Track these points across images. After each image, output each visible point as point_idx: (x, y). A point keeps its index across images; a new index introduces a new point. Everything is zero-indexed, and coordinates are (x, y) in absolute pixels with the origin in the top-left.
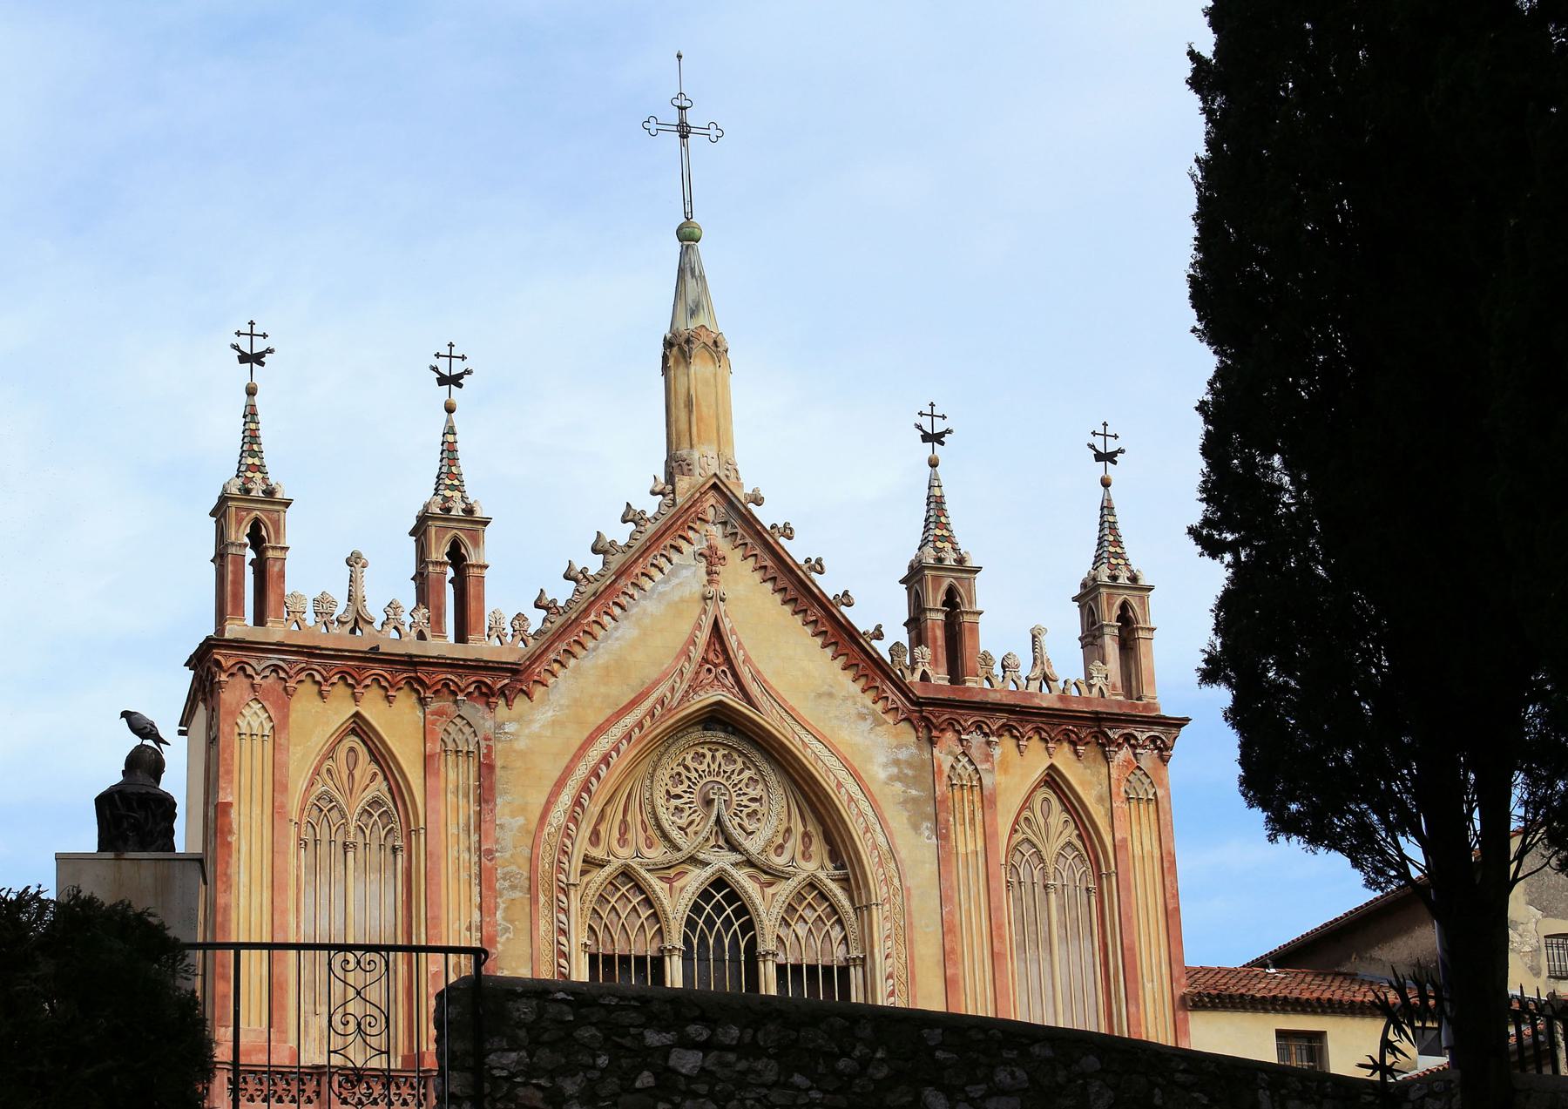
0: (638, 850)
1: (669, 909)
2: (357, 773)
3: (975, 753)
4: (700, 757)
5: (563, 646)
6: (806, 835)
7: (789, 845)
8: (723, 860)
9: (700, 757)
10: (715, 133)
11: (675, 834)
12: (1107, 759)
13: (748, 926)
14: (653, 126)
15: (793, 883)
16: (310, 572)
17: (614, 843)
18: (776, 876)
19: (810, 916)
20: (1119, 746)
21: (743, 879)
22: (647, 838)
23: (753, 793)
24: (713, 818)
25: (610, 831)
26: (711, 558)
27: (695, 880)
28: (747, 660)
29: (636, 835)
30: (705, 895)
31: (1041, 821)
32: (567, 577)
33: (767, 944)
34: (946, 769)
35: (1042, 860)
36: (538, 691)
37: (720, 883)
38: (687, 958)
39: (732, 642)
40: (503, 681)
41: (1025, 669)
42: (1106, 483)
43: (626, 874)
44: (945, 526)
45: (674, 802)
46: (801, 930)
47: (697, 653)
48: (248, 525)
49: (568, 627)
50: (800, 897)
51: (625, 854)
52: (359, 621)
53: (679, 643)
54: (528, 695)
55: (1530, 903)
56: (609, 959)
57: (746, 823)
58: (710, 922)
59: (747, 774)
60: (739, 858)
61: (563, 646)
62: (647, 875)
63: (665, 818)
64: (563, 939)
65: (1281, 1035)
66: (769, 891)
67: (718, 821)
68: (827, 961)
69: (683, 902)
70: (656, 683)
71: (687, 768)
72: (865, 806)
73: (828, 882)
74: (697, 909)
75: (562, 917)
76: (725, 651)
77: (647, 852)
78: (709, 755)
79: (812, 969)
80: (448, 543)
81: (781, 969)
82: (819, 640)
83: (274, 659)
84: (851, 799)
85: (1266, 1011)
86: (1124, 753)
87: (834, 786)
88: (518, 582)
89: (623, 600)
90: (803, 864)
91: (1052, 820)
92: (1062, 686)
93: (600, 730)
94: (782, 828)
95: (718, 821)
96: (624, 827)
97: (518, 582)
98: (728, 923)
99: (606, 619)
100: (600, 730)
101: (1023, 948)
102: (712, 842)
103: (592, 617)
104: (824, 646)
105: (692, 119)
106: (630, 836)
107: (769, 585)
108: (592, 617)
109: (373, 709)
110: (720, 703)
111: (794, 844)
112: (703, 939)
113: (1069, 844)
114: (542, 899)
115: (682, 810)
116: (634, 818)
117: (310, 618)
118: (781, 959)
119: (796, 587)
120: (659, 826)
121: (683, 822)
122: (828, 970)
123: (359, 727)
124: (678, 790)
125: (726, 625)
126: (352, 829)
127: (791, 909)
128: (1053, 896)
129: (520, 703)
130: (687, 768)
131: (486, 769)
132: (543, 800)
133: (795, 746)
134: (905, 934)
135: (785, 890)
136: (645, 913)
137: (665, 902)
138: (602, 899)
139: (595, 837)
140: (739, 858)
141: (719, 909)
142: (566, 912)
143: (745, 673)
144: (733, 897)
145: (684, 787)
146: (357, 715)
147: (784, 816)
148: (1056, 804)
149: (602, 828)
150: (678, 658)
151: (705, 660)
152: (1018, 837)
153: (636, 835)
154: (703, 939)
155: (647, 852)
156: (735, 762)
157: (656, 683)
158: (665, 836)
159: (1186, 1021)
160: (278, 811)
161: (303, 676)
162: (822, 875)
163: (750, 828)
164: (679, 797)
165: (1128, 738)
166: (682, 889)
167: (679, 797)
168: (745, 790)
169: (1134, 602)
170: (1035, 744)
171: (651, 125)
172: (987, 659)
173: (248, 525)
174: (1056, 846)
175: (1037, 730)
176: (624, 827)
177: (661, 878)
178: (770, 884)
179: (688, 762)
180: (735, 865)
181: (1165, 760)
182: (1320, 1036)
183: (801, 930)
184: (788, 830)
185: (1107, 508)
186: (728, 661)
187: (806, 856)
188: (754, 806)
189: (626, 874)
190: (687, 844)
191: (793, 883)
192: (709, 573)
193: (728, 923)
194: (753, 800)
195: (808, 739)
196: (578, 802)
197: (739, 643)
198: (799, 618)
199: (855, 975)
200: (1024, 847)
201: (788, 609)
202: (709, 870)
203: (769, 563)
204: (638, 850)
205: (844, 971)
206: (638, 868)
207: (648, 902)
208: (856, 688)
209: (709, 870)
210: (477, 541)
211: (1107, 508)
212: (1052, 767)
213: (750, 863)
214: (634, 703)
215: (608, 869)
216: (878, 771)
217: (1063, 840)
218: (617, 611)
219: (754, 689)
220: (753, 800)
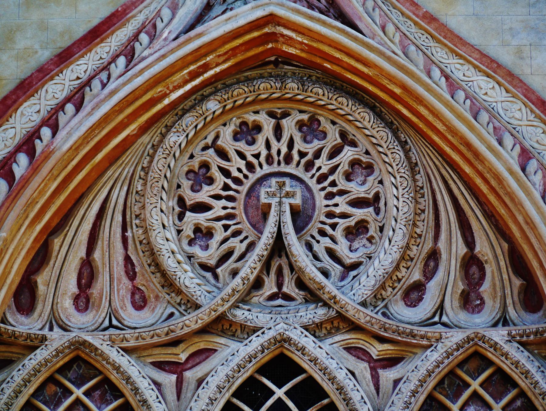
0: (112, 313)
4: (248, 132)
6: (472, 265)
8: (286, 324)
9: (248, 132)
11: (188, 279)
15: (434, 356)
17: (67, 303)
18: (400, 349)
21: (328, 359)
22: (135, 290)
23: (357, 189)
25: (59, 283)
27: (231, 361)
29: (112, 285)
37: (280, 365)
43: (80, 363)
45: (192, 218)
51: (82, 325)
57: (342, 247)
60: (317, 314)
62: (123, 360)
66: (387, 375)
67: (279, 247)
71: (223, 154)
73: (516, 353)
77: (131, 316)
78: (268, 124)
87: (513, 159)
90: (462, 317)
94: (419, 252)
95: (279, 247)
96: (87, 274)
102: (270, 287)
106: (102, 283)
111: (448, 276)
115: (209, 234)
116: (110, 256)
121: (210, 256)
124: (204, 195)
130: (223, 154)
133: (433, 94)
140: (317, 314)
145: (216, 188)
147: (425, 227)
149: (41, 280)
155: (131, 316)
156: (324, 135)
158: (169, 284)
162: (499, 335)
163: (350, 258)
166: (200, 382)
168: (343, 184)
176: (87, 274)
177: (159, 365)
178: (391, 362)
179: (226, 141)
180: (314, 329)
184: (434, 255)
187: (470, 301)
188: (359, 213)
190: (213, 301)
191: (434, 356)
195: (460, 70)
202: (256, 342)
204: (112, 313)
206: (105, 348)
209: (256, 342)
213: (342, 322)
215: (41, 355)
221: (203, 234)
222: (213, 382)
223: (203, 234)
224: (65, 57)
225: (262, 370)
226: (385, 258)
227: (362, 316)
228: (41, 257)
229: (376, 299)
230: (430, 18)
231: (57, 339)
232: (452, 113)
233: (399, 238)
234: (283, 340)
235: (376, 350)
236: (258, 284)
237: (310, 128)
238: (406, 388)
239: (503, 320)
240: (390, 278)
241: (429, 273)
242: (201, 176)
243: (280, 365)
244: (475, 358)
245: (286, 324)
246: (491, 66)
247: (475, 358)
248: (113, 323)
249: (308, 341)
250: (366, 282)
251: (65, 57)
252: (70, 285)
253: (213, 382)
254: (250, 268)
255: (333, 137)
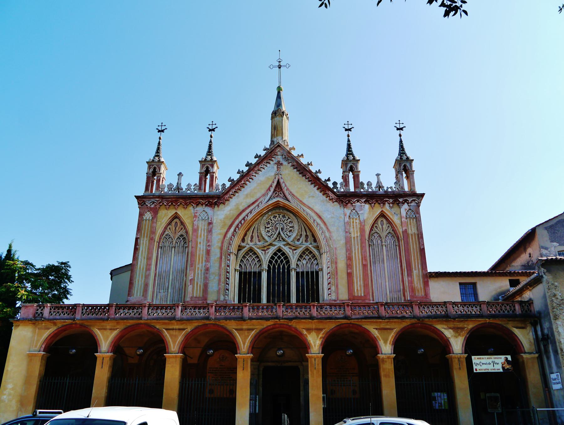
1: (263, 258)
2: (177, 228)
3: (357, 209)
5: (234, 190)
6: (307, 236)
7: (301, 239)
8: (281, 244)
9: (275, 217)
10: (288, 66)
11: (266, 238)
12: (400, 208)
13: (288, 262)
14: (272, 67)
15: (301, 249)
16: (168, 178)
19: (307, 258)
20: (404, 204)
21: (286, 249)
23: (290, 225)
24: (277, 232)
25: (248, 238)
26: (279, 164)
27: (272, 250)
28: (288, 189)
29: (256, 239)
30: (275, 254)
31: (381, 227)
32: (238, 173)
33: (293, 265)
34: (348, 214)
35: (381, 237)
36: (227, 203)
37: (279, 250)
38: (269, 272)
39: (283, 185)
40: (215, 200)
41: (374, 185)
42: (400, 135)
43: (251, 250)
44: (351, 151)
46: (304, 262)
47: (272, 190)
48: (154, 170)
49: (236, 185)
50: (304, 253)
51: (251, 244)
52: (178, 188)
53: (268, 186)
54: (224, 204)
55: (552, 242)
56: (245, 273)
57: (288, 233)
58: (276, 261)
59: (289, 220)
60: (285, 243)
61: (234, 190)
62: (257, 249)
63: (263, 233)
64: (228, 268)
65: (460, 284)
66: (295, 252)
67: (279, 233)
68: (312, 270)
69: (268, 256)
70: (260, 198)
72: (322, 225)
73: (313, 248)
74: (272, 258)
75: (228, 262)
76: (281, 188)
77: (258, 243)
78: (278, 216)
79: (307, 273)
80: (207, 167)
81: (297, 273)
82: (310, 183)
83: (153, 200)
84: (318, 224)
85: (455, 277)
86: (406, 206)
88: (223, 176)
89: (252, 177)
91: (384, 226)
92: (385, 189)
93: (243, 211)
95: (279, 233)
97: (223, 176)
98: (282, 261)
99: (247, 182)
100: (243, 211)
101: (375, 263)
102: (278, 239)
103: (243, 182)
104: (311, 184)
105: (281, 64)
106: (254, 238)
107: (295, 170)
108: (243, 182)
109: (181, 212)
110: (278, 201)
111: (303, 238)
112: (274, 266)
113: (389, 233)
114: (223, 257)
116: (255, 235)
117: (166, 190)
118: (298, 270)
119: (303, 170)
120: (262, 236)
121: (269, 235)
122: (312, 272)
123: (176, 216)
124: (268, 226)
125: (281, 181)
126: (174, 242)
127: (301, 256)
128: (384, 247)
129: (221, 206)
131: (210, 224)
132: (225, 230)
133: (301, 212)
134: (334, 262)
135: (299, 251)
136: (256, 260)
137: (262, 256)
138: (244, 257)
139: (243, 240)
140: (285, 243)
141: (279, 258)
142: (229, 260)
143: (287, 193)
144: (283, 254)
146: (176, 213)
148: (385, 221)
149: (245, 238)
150: (267, 190)
151: (275, 190)
152: (373, 232)
153: (256, 239)
154: (274, 266)
155: (258, 243)
157: (260, 198)
158: (264, 238)
159: (428, 282)
160: (152, 239)
161: (161, 204)
162: (310, 246)
164: (268, 228)
165: (406, 201)
167: (268, 228)
169: (408, 165)
170: (377, 205)
171: (271, 67)
172: (362, 184)
173: (154, 170)
174: (385, 234)
175: (377, 201)
178: (295, 250)
179: (272, 218)
180: (284, 245)
181: (419, 206)
182: (474, 285)
183: (304, 262)
184: (301, 235)
185: (401, 141)
186: (282, 190)
187: (306, 241)
189: (251, 250)
190: (269, 241)
191: (301, 249)
192: (277, 168)
193: (282, 261)
194: (291, 227)
196: (235, 230)
197: (285, 185)
198: (304, 178)
199: (320, 273)
200: (375, 235)
201: (301, 175)
202: (276, 247)
203: (295, 164)
205: (317, 273)
207: (258, 257)
208: (321, 194)
209: (276, 247)
210: (212, 166)
211: (401, 141)
212: (382, 211)
213: (288, 244)
214: (253, 203)
215: (245, 249)
216: (326, 216)
217: (388, 232)
218: (250, 180)
219: (289, 197)
220: (291, 227)
221: (268, 231)
222: (270, 252)
223: (268, 231)
224: (249, 206)
225: (277, 251)
226: (294, 235)
227: (291, 243)
228: (245, 235)
229: (293, 241)
230: (301, 201)
231: (248, 246)
232: (304, 214)
233: (296, 232)
234: (280, 247)
235: (293, 248)
236: (276, 239)
237: (284, 216)
238: (297, 253)
239: (311, 244)
240: (295, 238)
241: (300, 237)
242: (268, 223)
243: (279, 250)
244: (307, 249)
245: (281, 244)
246: (309, 208)
247: (307, 249)
248: (256, 244)
249: (283, 247)
250: (292, 239)
251: (249, 206)
252: (250, 239)
253: (270, 252)
254: (275, 236)
255: (287, 218)
